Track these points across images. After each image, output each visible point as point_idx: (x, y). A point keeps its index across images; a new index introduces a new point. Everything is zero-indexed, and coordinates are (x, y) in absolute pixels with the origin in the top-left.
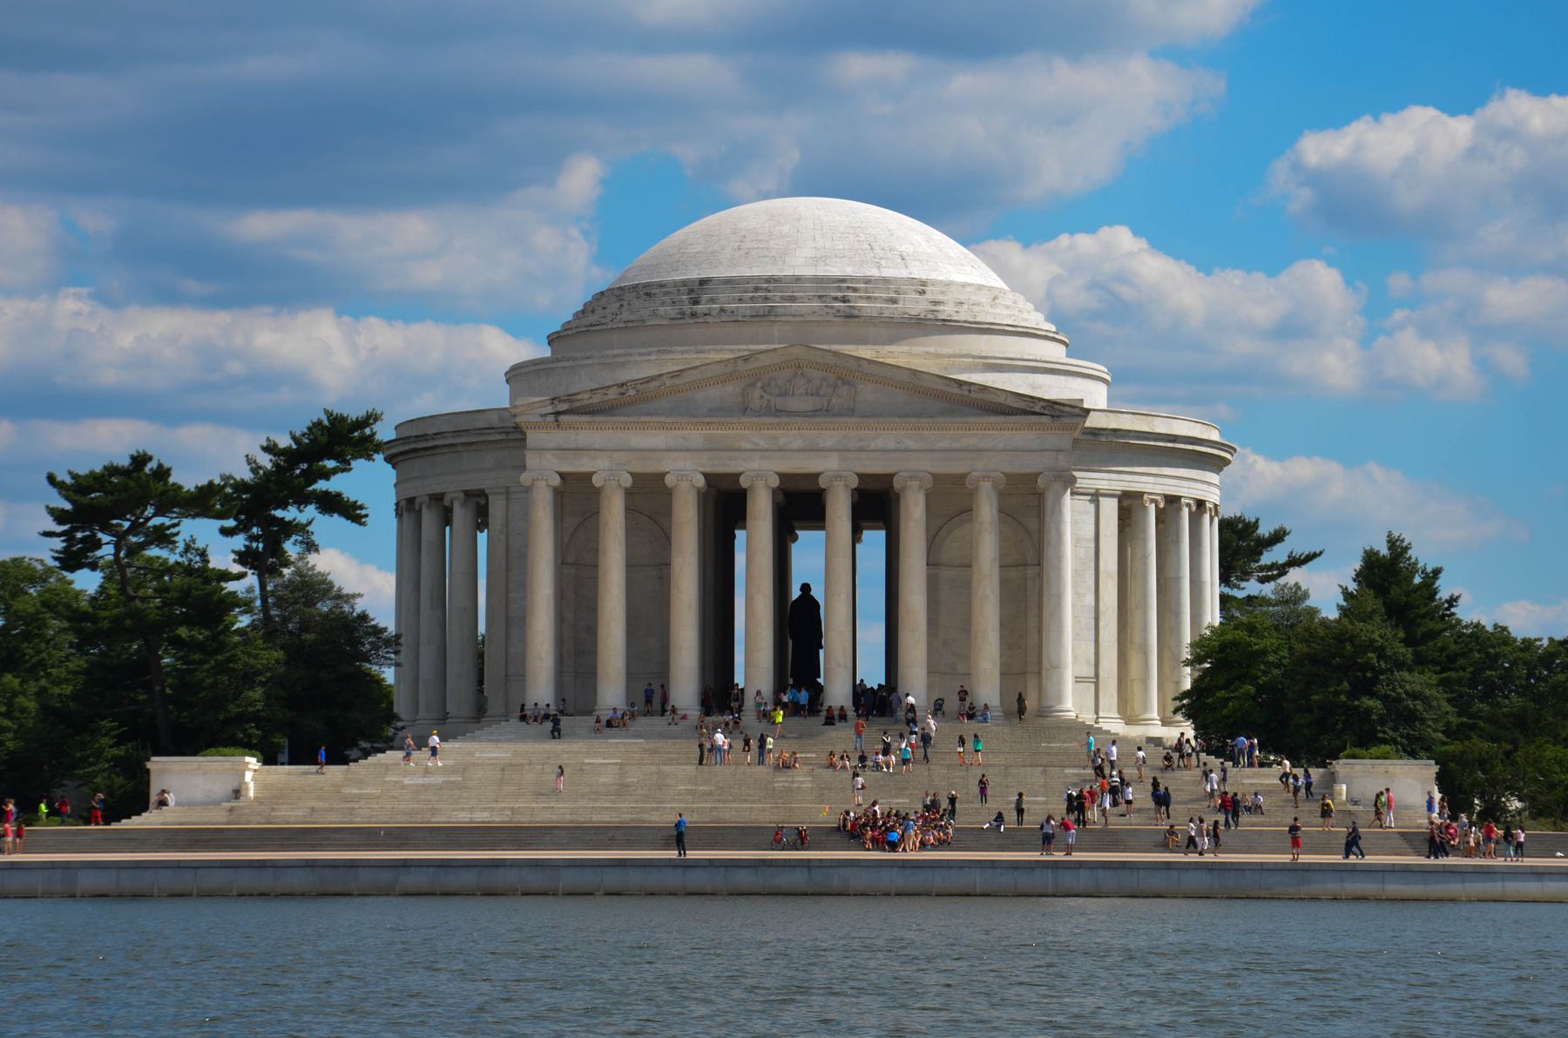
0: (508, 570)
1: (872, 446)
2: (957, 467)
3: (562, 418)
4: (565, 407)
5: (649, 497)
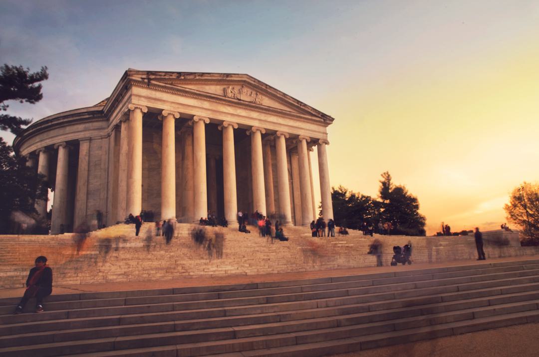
0: (89, 171)
1: (269, 120)
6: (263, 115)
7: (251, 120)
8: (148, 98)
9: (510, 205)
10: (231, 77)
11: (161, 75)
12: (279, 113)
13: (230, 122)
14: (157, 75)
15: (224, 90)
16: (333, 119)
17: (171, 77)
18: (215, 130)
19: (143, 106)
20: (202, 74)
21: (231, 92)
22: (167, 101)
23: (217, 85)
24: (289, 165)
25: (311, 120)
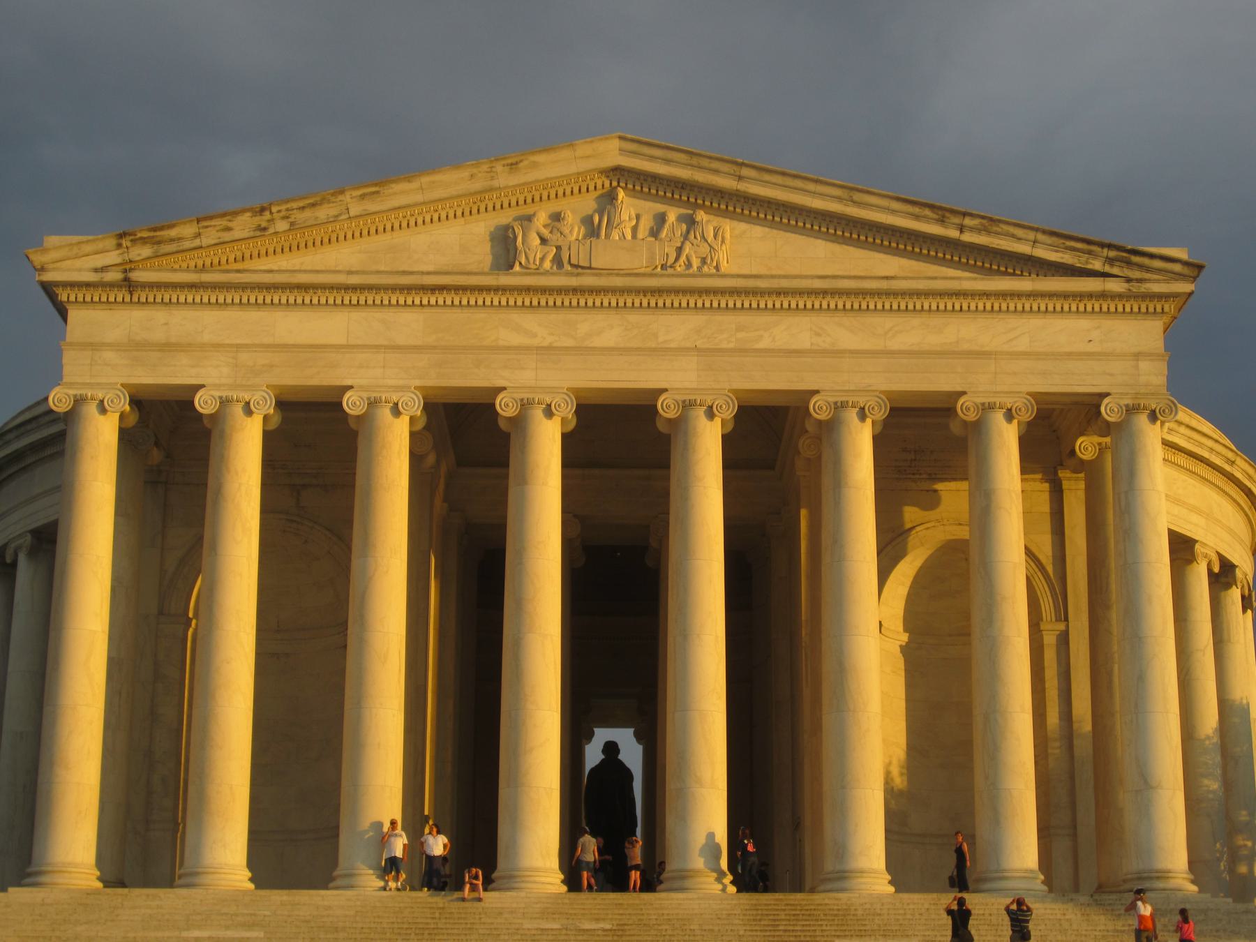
2: (937, 381)
6: (730, 320)
8: (135, 347)
11: (179, 239)
14: (159, 243)
16: (1200, 267)
17: (227, 236)
21: (544, 241)
22: (217, 347)
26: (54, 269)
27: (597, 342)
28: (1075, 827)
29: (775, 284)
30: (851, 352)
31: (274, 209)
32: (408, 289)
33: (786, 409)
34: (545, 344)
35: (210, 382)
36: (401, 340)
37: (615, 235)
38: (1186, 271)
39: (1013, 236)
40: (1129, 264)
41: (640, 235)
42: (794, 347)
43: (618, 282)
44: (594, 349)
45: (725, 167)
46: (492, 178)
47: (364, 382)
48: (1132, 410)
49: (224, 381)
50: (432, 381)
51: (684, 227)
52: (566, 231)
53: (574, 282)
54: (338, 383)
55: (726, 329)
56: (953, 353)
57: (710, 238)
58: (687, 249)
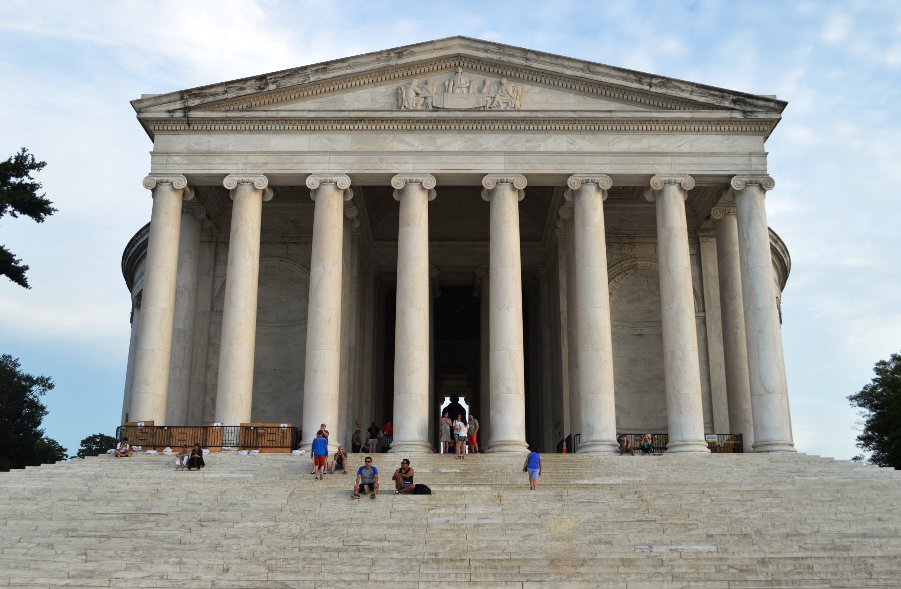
1: (541, 149)
2: (638, 168)
3: (194, 114)
4: (197, 101)
5: (290, 205)
6: (522, 137)
7: (478, 159)
8: (190, 154)
9: (17, 369)
10: (412, 53)
11: (215, 94)
12: (575, 120)
13: (412, 174)
14: (204, 96)
15: (398, 95)
16: (784, 104)
17: (242, 93)
18: (374, 206)
19: (177, 175)
20: (325, 66)
21: (417, 94)
23: (376, 83)
24: (696, 268)
25: (709, 121)
26: (146, 111)
27: (448, 148)
28: (713, 423)
29: (547, 114)
30: (590, 153)
31: (268, 77)
32: (342, 120)
33: (553, 187)
34: (419, 149)
35: (232, 172)
36: (339, 147)
37: (458, 91)
38: (777, 106)
39: (679, 88)
40: (745, 103)
41: (471, 91)
42: (558, 150)
43: (460, 114)
44: (446, 152)
45: (518, 54)
46: (390, 60)
47: (316, 171)
48: (749, 184)
49: (240, 171)
50: (355, 170)
51: (496, 87)
52: (430, 89)
53: (435, 114)
54: (303, 172)
55: (520, 142)
56: (648, 153)
57: (510, 92)
58: (498, 98)
